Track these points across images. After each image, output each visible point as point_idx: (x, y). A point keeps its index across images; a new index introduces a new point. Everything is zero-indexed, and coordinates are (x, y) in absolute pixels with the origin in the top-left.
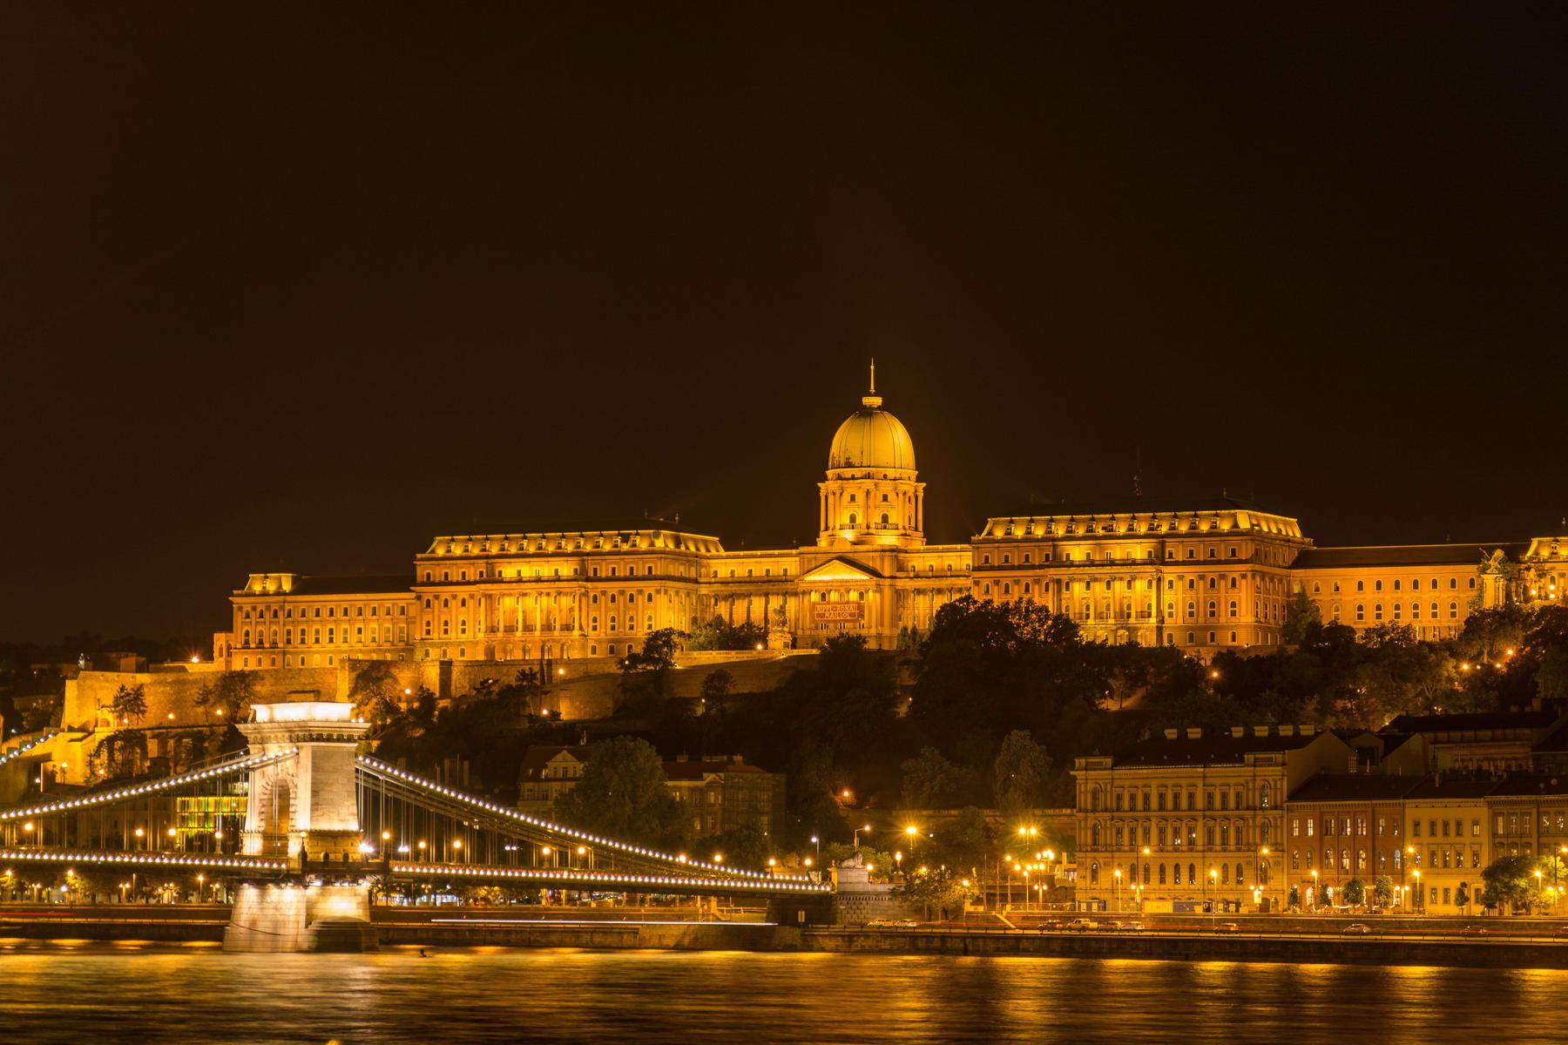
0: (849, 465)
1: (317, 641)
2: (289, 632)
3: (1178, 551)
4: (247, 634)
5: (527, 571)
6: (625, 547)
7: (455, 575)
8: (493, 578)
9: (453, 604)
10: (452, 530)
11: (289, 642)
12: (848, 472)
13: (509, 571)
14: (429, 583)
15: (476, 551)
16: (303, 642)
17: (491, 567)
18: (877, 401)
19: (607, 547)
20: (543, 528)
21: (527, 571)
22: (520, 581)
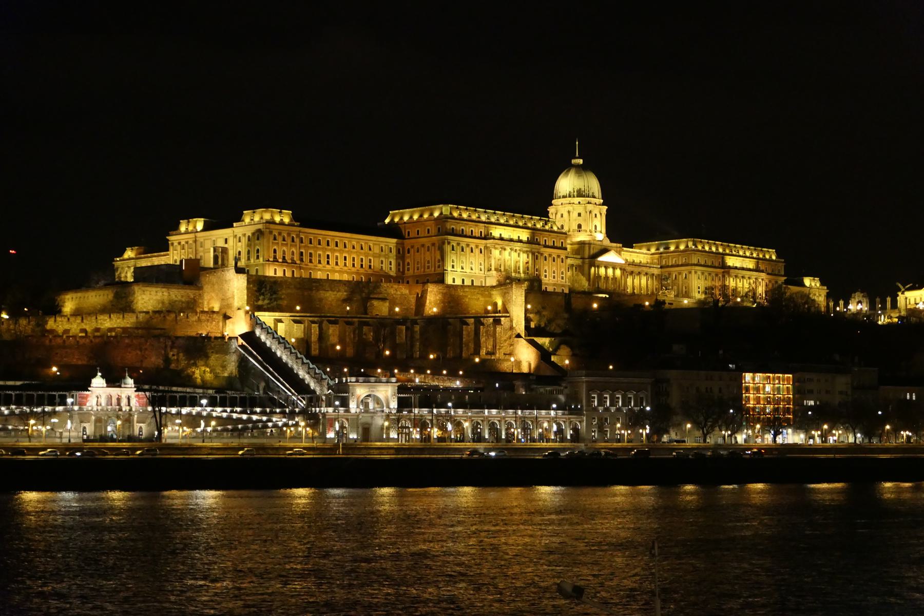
0: (594, 197)
1: (320, 262)
2: (301, 254)
3: (762, 267)
4: (275, 251)
5: (507, 233)
6: (547, 227)
7: (467, 229)
8: (487, 237)
9: (468, 250)
10: (457, 201)
11: (302, 260)
12: (593, 200)
13: (496, 232)
14: (453, 233)
15: (474, 217)
16: (311, 261)
17: (487, 229)
18: (581, 161)
19: (539, 226)
20: (505, 209)
21: (507, 233)
22: (501, 239)
